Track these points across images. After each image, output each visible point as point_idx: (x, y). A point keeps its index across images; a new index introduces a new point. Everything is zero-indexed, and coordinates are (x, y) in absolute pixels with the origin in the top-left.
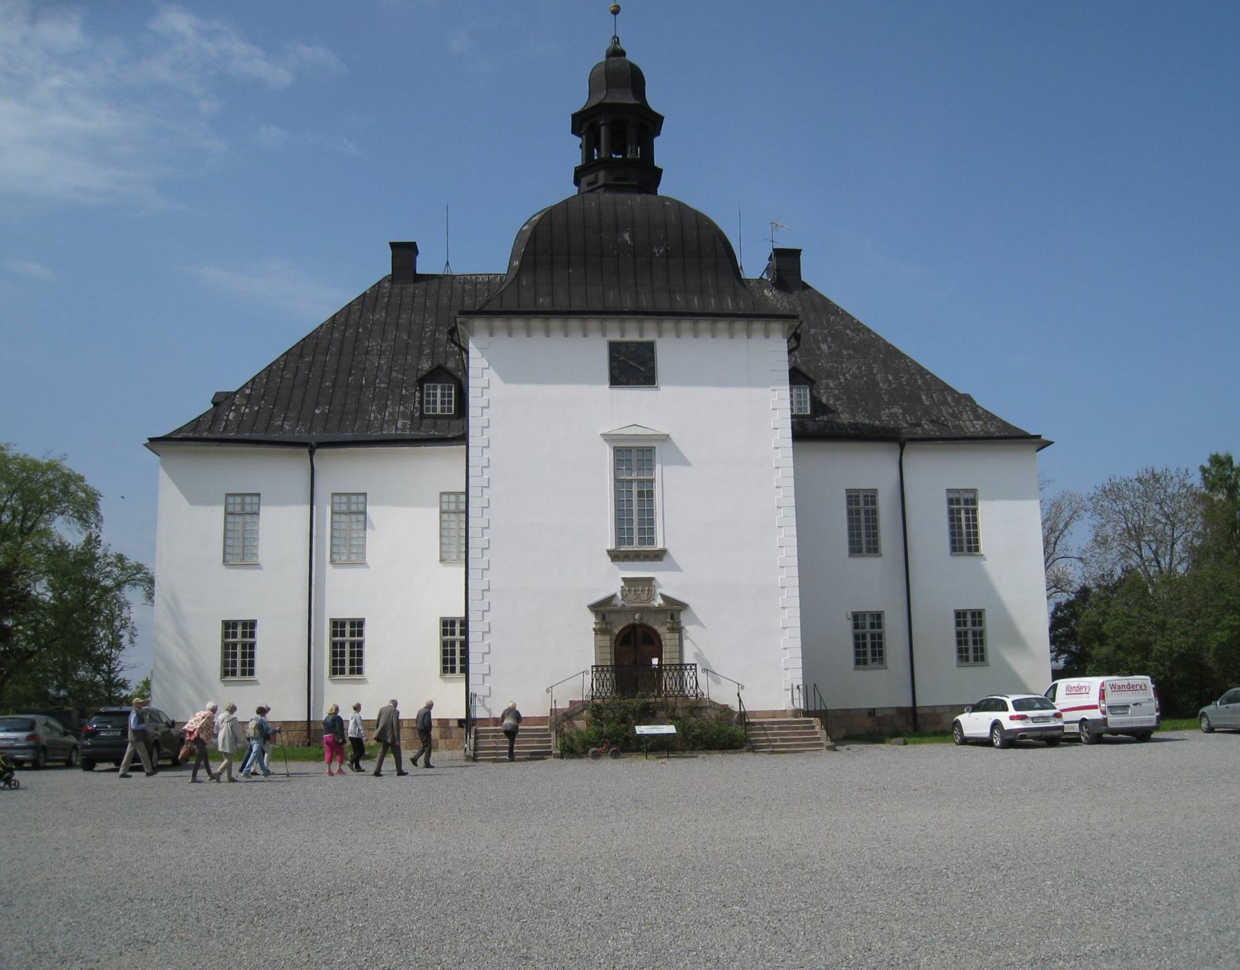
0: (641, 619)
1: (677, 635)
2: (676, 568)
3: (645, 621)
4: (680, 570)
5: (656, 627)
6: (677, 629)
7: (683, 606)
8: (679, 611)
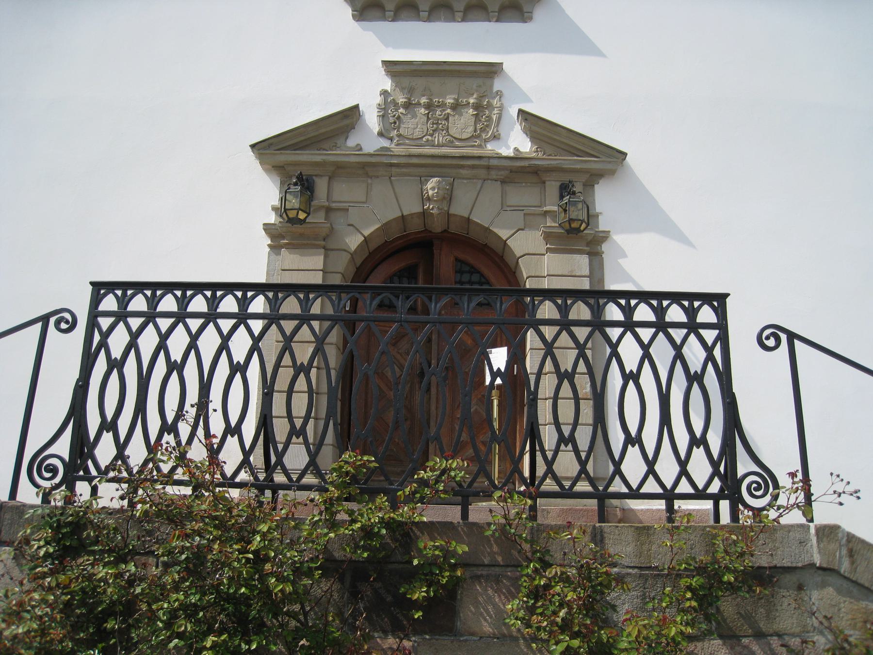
0: (448, 197)
2: (578, 43)
3: (460, 209)
4: (596, 52)
5: (503, 234)
6: (580, 234)
7: (607, 160)
8: (593, 178)
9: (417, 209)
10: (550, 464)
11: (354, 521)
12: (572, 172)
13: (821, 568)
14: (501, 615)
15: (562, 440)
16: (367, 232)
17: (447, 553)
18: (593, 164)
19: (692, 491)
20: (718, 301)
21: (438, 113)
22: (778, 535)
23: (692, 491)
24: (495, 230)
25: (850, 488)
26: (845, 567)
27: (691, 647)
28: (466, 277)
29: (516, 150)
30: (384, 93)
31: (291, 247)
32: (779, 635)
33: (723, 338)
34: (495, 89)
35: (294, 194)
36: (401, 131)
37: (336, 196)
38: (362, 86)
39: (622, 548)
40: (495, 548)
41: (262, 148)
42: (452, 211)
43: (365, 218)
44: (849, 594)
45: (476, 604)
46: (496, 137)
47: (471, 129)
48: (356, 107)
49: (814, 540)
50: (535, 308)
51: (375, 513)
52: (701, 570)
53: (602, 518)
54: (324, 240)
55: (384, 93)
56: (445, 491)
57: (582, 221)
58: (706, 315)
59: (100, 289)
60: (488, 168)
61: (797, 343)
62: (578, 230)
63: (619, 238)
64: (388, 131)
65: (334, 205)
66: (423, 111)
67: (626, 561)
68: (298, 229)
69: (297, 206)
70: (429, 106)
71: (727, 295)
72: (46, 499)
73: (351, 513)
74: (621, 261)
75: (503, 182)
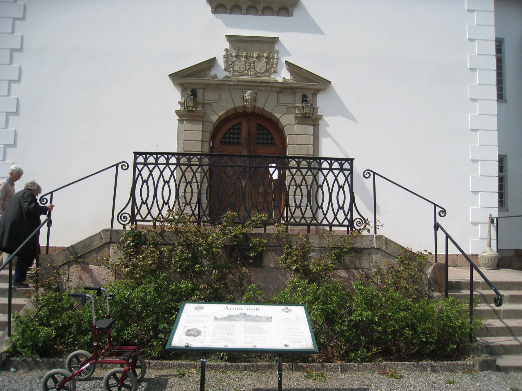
0: (254, 99)
1: (310, 129)
2: (313, 28)
3: (260, 104)
4: (321, 32)
5: (278, 116)
6: (310, 118)
9: (242, 104)
10: (292, 214)
11: (231, 233)
12: (308, 88)
13: (376, 248)
14: (276, 262)
15: (296, 207)
16: (220, 114)
17: (261, 243)
18: (316, 86)
19: (338, 224)
20: (351, 161)
21: (250, 60)
22: (364, 238)
23: (338, 224)
24: (275, 114)
25: (380, 224)
26: (384, 248)
27: (335, 272)
28: (261, 132)
29: (284, 78)
30: (226, 50)
31: (188, 120)
32: (362, 269)
33: (352, 173)
34: (275, 50)
35: (191, 100)
36: (234, 68)
37: (206, 98)
38: (217, 49)
39: (315, 241)
40: (275, 241)
41: (174, 77)
42: (256, 105)
43: (219, 108)
44: (385, 256)
45: (269, 258)
46: (275, 72)
47: (265, 68)
48: (215, 58)
49: (375, 240)
50: (289, 163)
51: (238, 230)
52: (338, 248)
53: (309, 232)
54: (202, 117)
55: (226, 50)
56: (260, 224)
57: (310, 114)
58: (346, 166)
59: (137, 154)
60: (272, 87)
61: (376, 175)
62: (308, 117)
63: (326, 118)
64: (228, 68)
65: (206, 102)
66: (243, 59)
67: (315, 245)
68: (192, 113)
69: (192, 105)
70: (246, 57)
71: (354, 159)
72: (124, 228)
73: (230, 231)
74: (327, 128)
75: (278, 92)
